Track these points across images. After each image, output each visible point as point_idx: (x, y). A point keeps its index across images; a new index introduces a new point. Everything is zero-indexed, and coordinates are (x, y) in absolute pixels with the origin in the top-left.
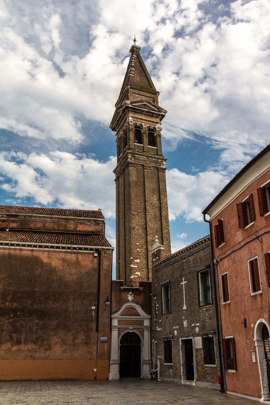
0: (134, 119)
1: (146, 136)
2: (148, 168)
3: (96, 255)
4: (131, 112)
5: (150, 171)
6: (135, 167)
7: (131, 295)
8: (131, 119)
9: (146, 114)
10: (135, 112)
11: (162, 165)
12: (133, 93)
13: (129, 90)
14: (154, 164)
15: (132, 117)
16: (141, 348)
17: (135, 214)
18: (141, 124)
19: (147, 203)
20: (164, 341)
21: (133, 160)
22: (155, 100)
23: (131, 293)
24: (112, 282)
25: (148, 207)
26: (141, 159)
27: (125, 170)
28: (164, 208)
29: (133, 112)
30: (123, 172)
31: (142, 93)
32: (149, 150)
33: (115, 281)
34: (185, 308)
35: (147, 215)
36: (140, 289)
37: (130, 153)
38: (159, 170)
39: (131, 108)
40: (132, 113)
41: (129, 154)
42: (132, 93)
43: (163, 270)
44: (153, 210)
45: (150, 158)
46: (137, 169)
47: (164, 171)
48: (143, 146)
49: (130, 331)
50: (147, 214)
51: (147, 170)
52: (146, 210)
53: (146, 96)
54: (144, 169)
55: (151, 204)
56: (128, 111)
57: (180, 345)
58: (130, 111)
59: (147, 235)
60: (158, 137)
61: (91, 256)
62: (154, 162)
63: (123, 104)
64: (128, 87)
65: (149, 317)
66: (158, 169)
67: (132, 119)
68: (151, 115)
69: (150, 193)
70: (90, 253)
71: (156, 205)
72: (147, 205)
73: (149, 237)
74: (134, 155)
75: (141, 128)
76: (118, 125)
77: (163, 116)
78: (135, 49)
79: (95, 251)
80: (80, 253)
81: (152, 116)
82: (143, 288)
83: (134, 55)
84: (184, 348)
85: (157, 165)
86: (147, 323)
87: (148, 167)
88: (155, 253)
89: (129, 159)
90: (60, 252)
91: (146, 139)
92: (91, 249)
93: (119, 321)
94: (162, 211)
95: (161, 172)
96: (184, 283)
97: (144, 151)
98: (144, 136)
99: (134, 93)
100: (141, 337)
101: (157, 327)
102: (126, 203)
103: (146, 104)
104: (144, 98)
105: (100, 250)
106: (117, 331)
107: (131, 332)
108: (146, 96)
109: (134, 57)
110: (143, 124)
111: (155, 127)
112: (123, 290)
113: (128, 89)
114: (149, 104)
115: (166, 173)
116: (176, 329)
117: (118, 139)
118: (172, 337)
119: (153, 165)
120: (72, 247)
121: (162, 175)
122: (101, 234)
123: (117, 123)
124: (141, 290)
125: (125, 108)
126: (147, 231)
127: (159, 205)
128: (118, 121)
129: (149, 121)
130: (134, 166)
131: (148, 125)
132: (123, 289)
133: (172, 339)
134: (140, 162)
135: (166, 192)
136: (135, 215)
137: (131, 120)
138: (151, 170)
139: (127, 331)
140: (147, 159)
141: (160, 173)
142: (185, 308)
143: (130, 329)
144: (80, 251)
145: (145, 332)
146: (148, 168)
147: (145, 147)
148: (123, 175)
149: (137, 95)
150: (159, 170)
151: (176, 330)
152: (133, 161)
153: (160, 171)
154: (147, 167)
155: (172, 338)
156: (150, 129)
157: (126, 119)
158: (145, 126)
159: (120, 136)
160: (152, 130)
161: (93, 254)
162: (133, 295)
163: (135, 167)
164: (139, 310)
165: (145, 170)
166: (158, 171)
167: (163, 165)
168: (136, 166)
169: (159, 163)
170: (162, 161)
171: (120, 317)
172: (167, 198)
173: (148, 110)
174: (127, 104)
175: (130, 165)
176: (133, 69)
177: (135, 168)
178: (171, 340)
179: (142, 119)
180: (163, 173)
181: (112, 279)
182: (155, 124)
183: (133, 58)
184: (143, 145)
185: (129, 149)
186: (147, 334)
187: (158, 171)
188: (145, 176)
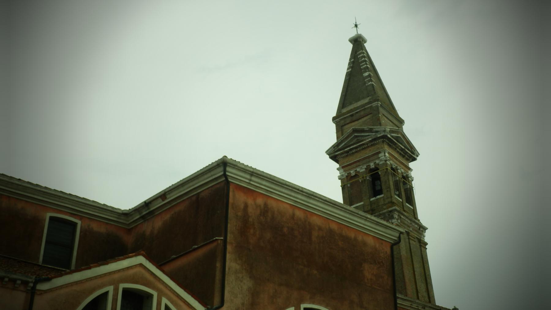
15: (389, 153)
26: (406, 222)
37: (399, 212)
41: (396, 213)
74: (400, 215)
173: (403, 148)
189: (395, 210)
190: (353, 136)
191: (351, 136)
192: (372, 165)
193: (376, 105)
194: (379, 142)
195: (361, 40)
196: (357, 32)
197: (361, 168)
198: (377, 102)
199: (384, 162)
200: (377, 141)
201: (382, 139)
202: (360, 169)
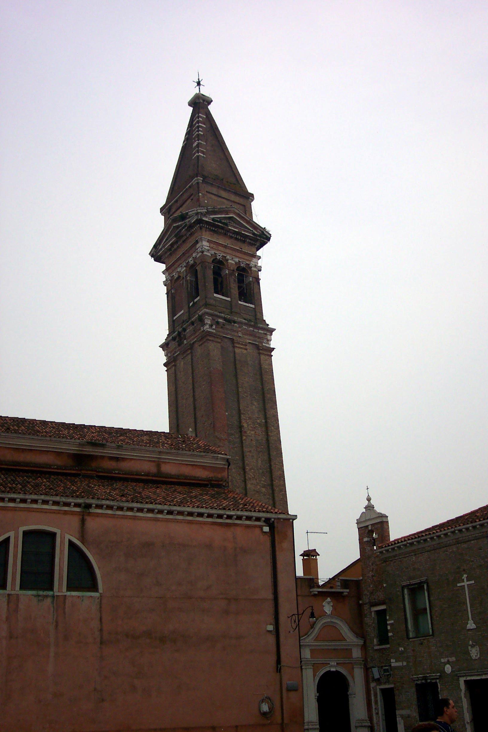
0: (212, 245)
1: (235, 281)
2: (242, 346)
3: (266, 529)
4: (206, 231)
5: (245, 351)
6: (219, 343)
7: (329, 603)
8: (205, 243)
11: (265, 341)
15: (208, 241)
16: (350, 698)
18: (226, 257)
20: (417, 685)
21: (214, 329)
22: (248, 210)
23: (329, 599)
24: (297, 579)
25: (245, 425)
27: (196, 345)
28: (273, 428)
29: (209, 231)
30: (190, 351)
31: (223, 194)
32: (240, 310)
33: (300, 578)
34: (471, 625)
36: (343, 592)
38: (261, 351)
39: (207, 222)
41: (207, 317)
42: (206, 193)
43: (405, 559)
44: (253, 430)
45: (244, 327)
46: (222, 347)
47: (269, 353)
48: (231, 302)
49: (333, 669)
50: (244, 438)
51: (240, 350)
54: (234, 347)
55: (250, 418)
57: (461, 690)
58: (204, 229)
59: (245, 481)
60: (256, 285)
61: (257, 531)
62: (251, 335)
63: (191, 213)
64: (198, 180)
65: (361, 642)
66: (259, 349)
67: (208, 244)
68: (241, 240)
69: (247, 396)
70: (256, 526)
72: (243, 421)
73: (249, 486)
74: (215, 318)
75: (223, 264)
76: (171, 250)
78: (202, 101)
79: (264, 521)
81: (244, 242)
82: (348, 590)
83: (200, 115)
84: (468, 695)
85: (255, 341)
86: (357, 653)
87: (242, 344)
88: (367, 526)
89: (208, 326)
90: (205, 523)
92: (258, 519)
93: (312, 651)
94: (269, 434)
95: (265, 355)
96: (466, 583)
97: (232, 312)
98: (232, 280)
99: (209, 193)
100: (349, 678)
101: (393, 660)
102: (199, 414)
104: (226, 205)
105: (273, 520)
106: (312, 670)
107: (333, 671)
109: (201, 117)
110: (228, 257)
111: (249, 265)
112: (315, 595)
113: (198, 183)
114: (239, 217)
115: (272, 357)
116: (448, 662)
117: (171, 280)
118: (440, 676)
119: (248, 340)
120: (225, 514)
122: (224, 484)
123: (170, 247)
124: (345, 594)
125: (194, 222)
126: (245, 472)
127: (263, 421)
128: (172, 245)
131: (237, 260)
132: (317, 593)
133: (438, 681)
134: (227, 334)
137: (207, 248)
138: (246, 349)
139: (328, 669)
141: (262, 357)
142: (471, 625)
143: (332, 666)
145: (355, 669)
146: (242, 346)
148: (189, 356)
149: (213, 197)
150: (261, 351)
151: (449, 664)
152: (214, 331)
153: (263, 354)
155: (437, 679)
156: (240, 267)
157: (197, 242)
158: (232, 261)
159: (176, 276)
160: (244, 270)
161: (261, 527)
162: (332, 604)
163: (219, 343)
164: (345, 630)
166: (259, 354)
168: (220, 341)
169: (259, 338)
170: (266, 334)
171: (314, 644)
176: (202, 142)
177: (219, 344)
178: (436, 683)
179: (225, 247)
180: (267, 357)
181: (297, 575)
183: (200, 119)
184: (229, 299)
185: (206, 305)
186: (359, 674)
188: (237, 362)
189: (204, 314)
190: (172, 227)
191: (170, 228)
192: (191, 261)
193: (197, 181)
194: (196, 229)
195: (202, 101)
196: (200, 91)
197: (181, 267)
198: (196, 178)
199: (200, 254)
200: (194, 229)
201: (199, 225)
202: (181, 268)
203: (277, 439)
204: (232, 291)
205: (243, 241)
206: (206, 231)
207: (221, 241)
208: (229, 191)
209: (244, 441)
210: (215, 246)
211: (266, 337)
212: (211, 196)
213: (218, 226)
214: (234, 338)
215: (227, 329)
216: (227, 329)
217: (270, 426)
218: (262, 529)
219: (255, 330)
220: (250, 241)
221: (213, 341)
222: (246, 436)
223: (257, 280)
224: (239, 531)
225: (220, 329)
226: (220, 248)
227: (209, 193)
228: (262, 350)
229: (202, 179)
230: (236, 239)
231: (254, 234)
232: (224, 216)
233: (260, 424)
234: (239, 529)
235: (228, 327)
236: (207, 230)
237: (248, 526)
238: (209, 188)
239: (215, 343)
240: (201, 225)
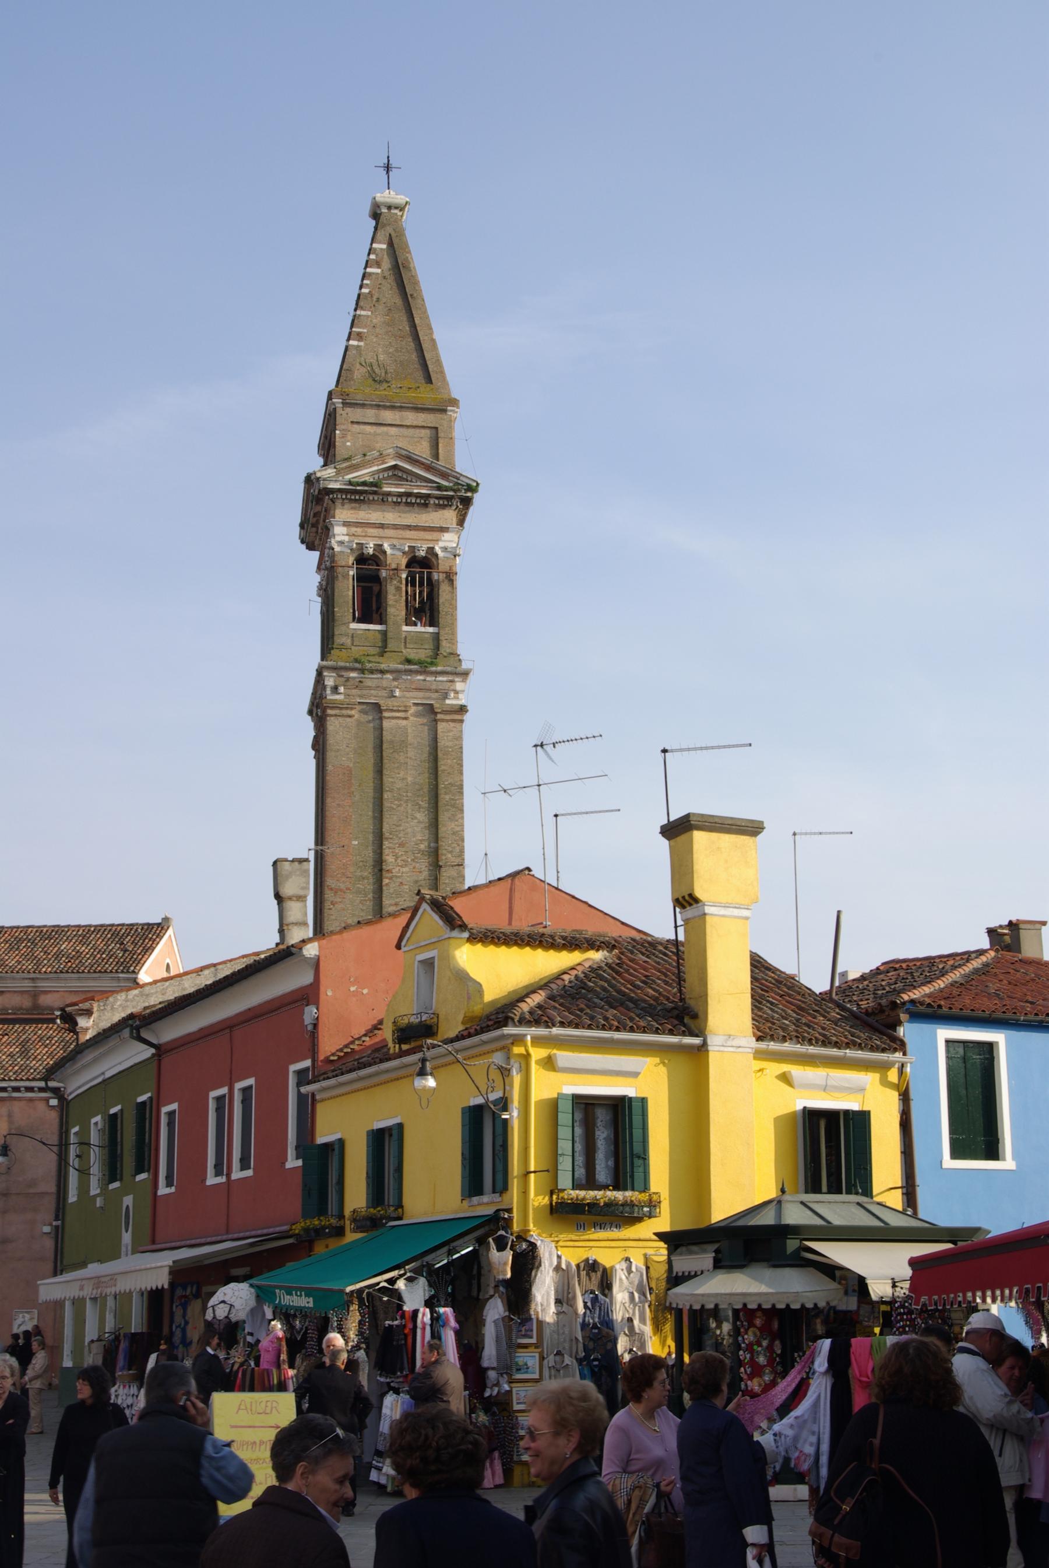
0: (353, 530)
1: (398, 589)
3: (54, 1102)
4: (343, 504)
9: (399, 503)
10: (356, 501)
12: (352, 422)
13: (339, 411)
14: (421, 694)
15: (346, 524)
17: (342, 886)
18: (381, 545)
19: (386, 844)
35: (387, 884)
37: (328, 668)
39: (340, 490)
40: (346, 506)
45: (404, 677)
50: (386, 881)
51: (395, 721)
52: (381, 870)
53: (408, 427)
55: (402, 845)
56: (333, 501)
58: (338, 503)
61: (41, 1106)
68: (418, 504)
71: (422, 847)
72: (386, 851)
77: (467, 502)
80: (15, 1099)
81: (426, 505)
85: (429, 698)
87: (398, 711)
91: (396, 604)
95: (447, 721)
99: (358, 423)
103: (396, 465)
108: (408, 427)
110: (386, 546)
121: (449, 731)
127: (432, 845)
129: (409, 527)
130: (344, 712)
135: (462, 793)
136: (341, 890)
140: (394, 679)
141: (441, 726)
144: (16, 1094)
147: (389, 635)
149: (368, 428)
150: (439, 716)
153: (443, 720)
154: (392, 711)
156: (415, 557)
161: (47, 1100)
165: (386, 724)
167: (457, 692)
172: (463, 818)
174: (324, 480)
175: (329, 712)
179: (382, 526)
180: (452, 724)
182: (434, 535)
187: (436, 721)
188: (385, 746)
203: (455, 875)
204: (391, 610)
205: (423, 504)
206: (343, 504)
207: (375, 515)
208: (401, 407)
209: (384, 888)
210: (359, 530)
211: (452, 688)
212: (362, 427)
213: (361, 492)
214: (381, 702)
215: (370, 688)
216: (370, 688)
217: (444, 852)
218: (48, 1102)
219: (428, 679)
220: (437, 502)
221: (336, 715)
222: (391, 878)
223: (450, 577)
224: (17, 1107)
225: (354, 692)
226: (372, 531)
227: (358, 423)
228: (440, 713)
229: (340, 401)
230: (407, 504)
231: (439, 488)
232: (375, 468)
233: (422, 852)
234: (16, 1103)
235: (368, 683)
236: (346, 501)
237: (31, 1100)
238: (357, 414)
239: (341, 719)
240: (331, 496)
